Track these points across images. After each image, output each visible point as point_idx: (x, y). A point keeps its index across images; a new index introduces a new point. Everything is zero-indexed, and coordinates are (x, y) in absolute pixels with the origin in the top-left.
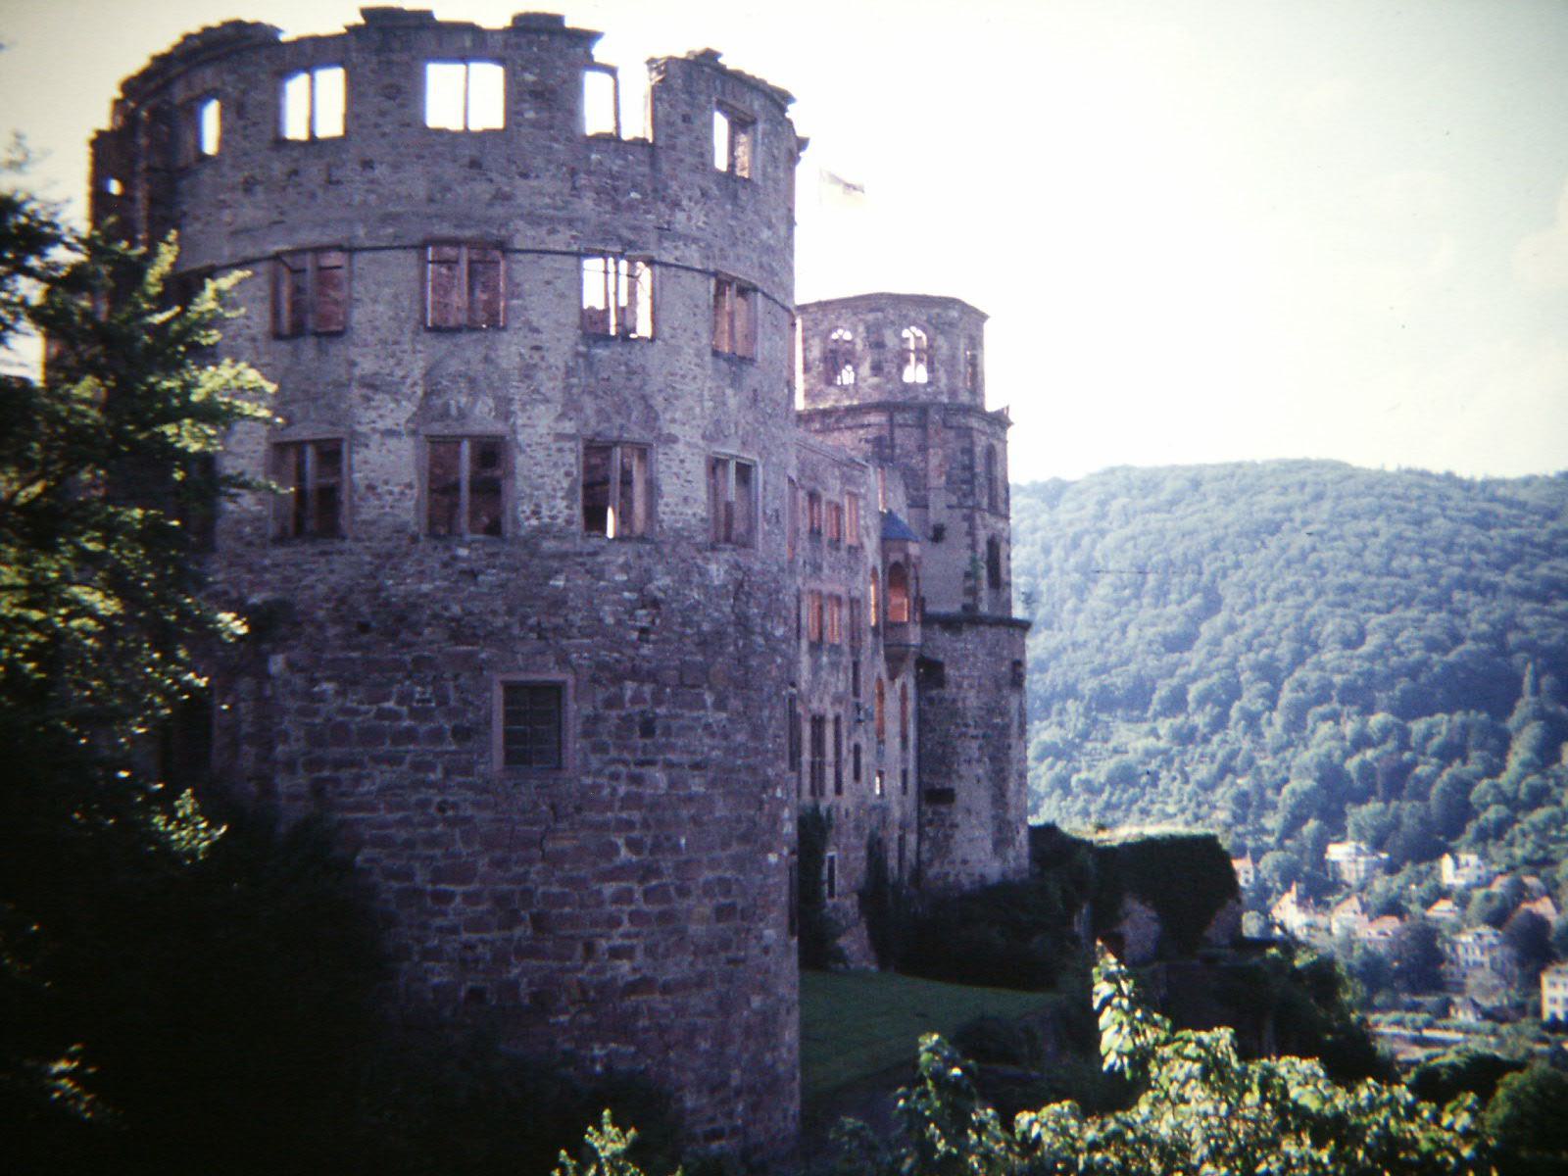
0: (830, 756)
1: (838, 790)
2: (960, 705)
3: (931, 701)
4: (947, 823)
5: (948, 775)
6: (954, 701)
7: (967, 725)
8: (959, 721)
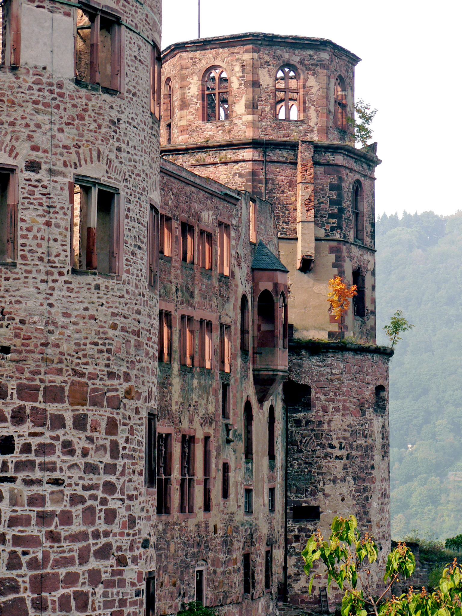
0: (199, 475)
2: (325, 426)
3: (298, 423)
5: (313, 494)
6: (320, 423)
7: (332, 446)
8: (324, 441)
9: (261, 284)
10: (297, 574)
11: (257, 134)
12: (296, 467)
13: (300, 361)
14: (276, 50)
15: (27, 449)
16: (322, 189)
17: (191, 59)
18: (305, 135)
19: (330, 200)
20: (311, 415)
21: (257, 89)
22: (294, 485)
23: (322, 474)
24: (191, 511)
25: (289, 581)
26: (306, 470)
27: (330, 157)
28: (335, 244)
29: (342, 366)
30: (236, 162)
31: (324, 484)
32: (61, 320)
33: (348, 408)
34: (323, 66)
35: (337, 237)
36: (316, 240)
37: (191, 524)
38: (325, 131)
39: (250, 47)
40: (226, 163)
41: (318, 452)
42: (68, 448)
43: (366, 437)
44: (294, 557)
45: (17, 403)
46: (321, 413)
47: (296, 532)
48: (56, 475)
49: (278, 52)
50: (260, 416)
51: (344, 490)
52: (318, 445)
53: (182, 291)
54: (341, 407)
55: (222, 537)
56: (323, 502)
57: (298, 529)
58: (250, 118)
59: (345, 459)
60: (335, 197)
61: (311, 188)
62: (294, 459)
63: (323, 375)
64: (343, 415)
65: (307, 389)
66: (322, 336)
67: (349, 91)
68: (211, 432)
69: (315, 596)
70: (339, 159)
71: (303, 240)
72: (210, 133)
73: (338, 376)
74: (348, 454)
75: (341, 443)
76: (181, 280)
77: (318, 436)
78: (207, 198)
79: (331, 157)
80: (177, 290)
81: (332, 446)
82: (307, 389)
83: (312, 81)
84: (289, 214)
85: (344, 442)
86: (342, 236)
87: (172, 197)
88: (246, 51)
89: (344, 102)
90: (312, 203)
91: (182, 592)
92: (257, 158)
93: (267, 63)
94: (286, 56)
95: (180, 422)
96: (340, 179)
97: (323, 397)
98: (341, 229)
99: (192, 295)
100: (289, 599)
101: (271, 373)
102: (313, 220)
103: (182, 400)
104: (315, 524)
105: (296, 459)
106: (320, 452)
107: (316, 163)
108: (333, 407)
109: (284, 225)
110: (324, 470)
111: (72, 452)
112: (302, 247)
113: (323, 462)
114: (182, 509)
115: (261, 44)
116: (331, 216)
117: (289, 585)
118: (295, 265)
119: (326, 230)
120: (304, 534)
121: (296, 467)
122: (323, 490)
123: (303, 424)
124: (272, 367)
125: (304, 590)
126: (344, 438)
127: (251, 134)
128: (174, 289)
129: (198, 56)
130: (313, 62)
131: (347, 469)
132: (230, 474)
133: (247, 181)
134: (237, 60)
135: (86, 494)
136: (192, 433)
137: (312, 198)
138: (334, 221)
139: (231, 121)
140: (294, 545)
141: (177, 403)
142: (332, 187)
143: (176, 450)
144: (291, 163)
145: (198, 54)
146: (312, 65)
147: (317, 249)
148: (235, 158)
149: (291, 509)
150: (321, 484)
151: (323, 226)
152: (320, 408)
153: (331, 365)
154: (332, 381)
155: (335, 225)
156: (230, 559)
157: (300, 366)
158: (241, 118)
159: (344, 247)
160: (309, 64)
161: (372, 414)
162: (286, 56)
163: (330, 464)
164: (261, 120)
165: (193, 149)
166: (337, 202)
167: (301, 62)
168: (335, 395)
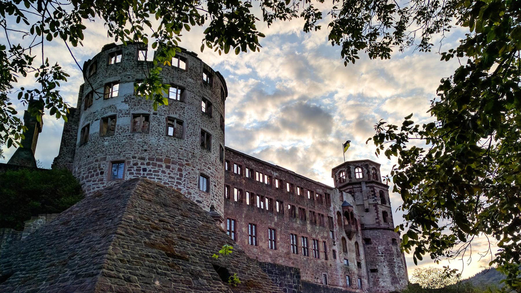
3: (368, 248)
5: (375, 266)
15: (150, 171)
32: (162, 145)
42: (163, 172)
45: (148, 161)
48: (160, 177)
50: (350, 244)
111: (165, 173)
135: (170, 183)
142: (372, 191)
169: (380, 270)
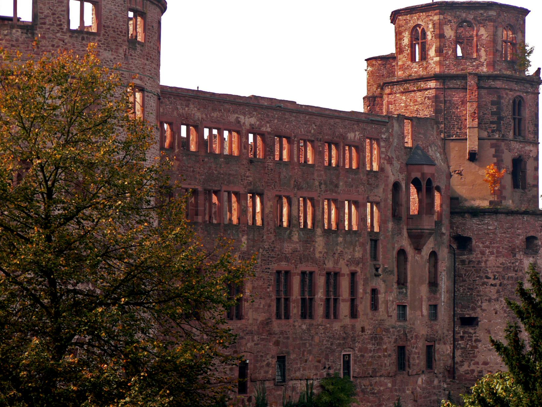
1: (354, 314)
2: (483, 264)
3: (463, 262)
4: (474, 339)
5: (474, 309)
6: (479, 262)
7: (487, 278)
8: (482, 274)
9: (412, 174)
10: (462, 362)
11: (442, 69)
12: (462, 291)
13: (464, 221)
14: (456, 12)
16: (485, 105)
17: (405, 20)
18: (477, 68)
19: (492, 112)
20: (473, 257)
21: (442, 39)
22: (460, 303)
23: (480, 296)
24: (336, 316)
25: (456, 366)
26: (468, 293)
27: (492, 83)
28: (495, 141)
29: (496, 224)
30: (427, 89)
31: (482, 303)
33: (501, 252)
34: (491, 20)
35: (497, 136)
36: (479, 139)
37: (337, 326)
38: (492, 64)
39: (437, 11)
40: (420, 90)
41: (477, 282)
43: (516, 271)
44: (460, 350)
46: (479, 256)
47: (462, 334)
49: (458, 13)
51: (497, 306)
52: (477, 277)
53: (325, 184)
54: (495, 251)
55: (370, 334)
56: (481, 315)
57: (463, 332)
58: (437, 59)
59: (498, 286)
60: (495, 110)
61: (475, 105)
62: (460, 286)
63: (481, 230)
64: (497, 257)
65: (469, 239)
66: (485, 204)
67: (520, 35)
68: (358, 270)
69: (475, 376)
70: (498, 84)
71: (470, 140)
72: (415, 69)
73: (492, 231)
74: (501, 283)
75: (495, 276)
76: (324, 177)
77: (477, 271)
78: (353, 124)
79: (493, 83)
80: (320, 184)
81: (487, 278)
82: (469, 239)
83: (482, 31)
84: (462, 123)
85: (497, 274)
86: (501, 136)
87: (315, 127)
88: (436, 14)
89: (514, 42)
90: (476, 115)
91: (327, 367)
92: (438, 87)
93: (450, 21)
94: (464, 15)
95: (325, 264)
96: (500, 97)
97: (481, 245)
98: (500, 131)
99: (337, 186)
100: (456, 378)
101: (419, 231)
102: (477, 126)
103: (326, 251)
104: (475, 329)
105: (462, 286)
106: (478, 281)
107: (479, 87)
108: (489, 252)
109: (458, 131)
110: (482, 293)
112: (472, 144)
113: (481, 288)
114: (327, 316)
115: (445, 9)
116: (492, 123)
117: (457, 368)
118: (465, 156)
119: (488, 132)
120: (467, 335)
121: (462, 291)
122: (481, 306)
123: (467, 263)
124: (420, 227)
125: (467, 372)
126: (497, 272)
127: (438, 70)
128: (317, 183)
129: (408, 18)
130: (483, 18)
131: (500, 292)
132: (379, 296)
133: (432, 102)
134: (430, 20)
136: (337, 270)
137: (476, 112)
138: (494, 126)
139: (427, 61)
140: (460, 342)
141: (320, 252)
143: (321, 281)
144: (462, 88)
145: (408, 17)
146: (483, 20)
147: (479, 145)
148: (425, 87)
149: (457, 319)
150: (480, 303)
151: (486, 129)
152: (479, 252)
153: (487, 223)
154: (488, 234)
155: (495, 129)
156: (379, 348)
157: (465, 224)
158: (433, 59)
159: (503, 144)
160: (480, 20)
161: (522, 256)
162: (464, 15)
163: (486, 290)
164: (446, 60)
165: (401, 81)
166: (497, 113)
167: (474, 19)
168: (491, 243)
169: (483, 322)
